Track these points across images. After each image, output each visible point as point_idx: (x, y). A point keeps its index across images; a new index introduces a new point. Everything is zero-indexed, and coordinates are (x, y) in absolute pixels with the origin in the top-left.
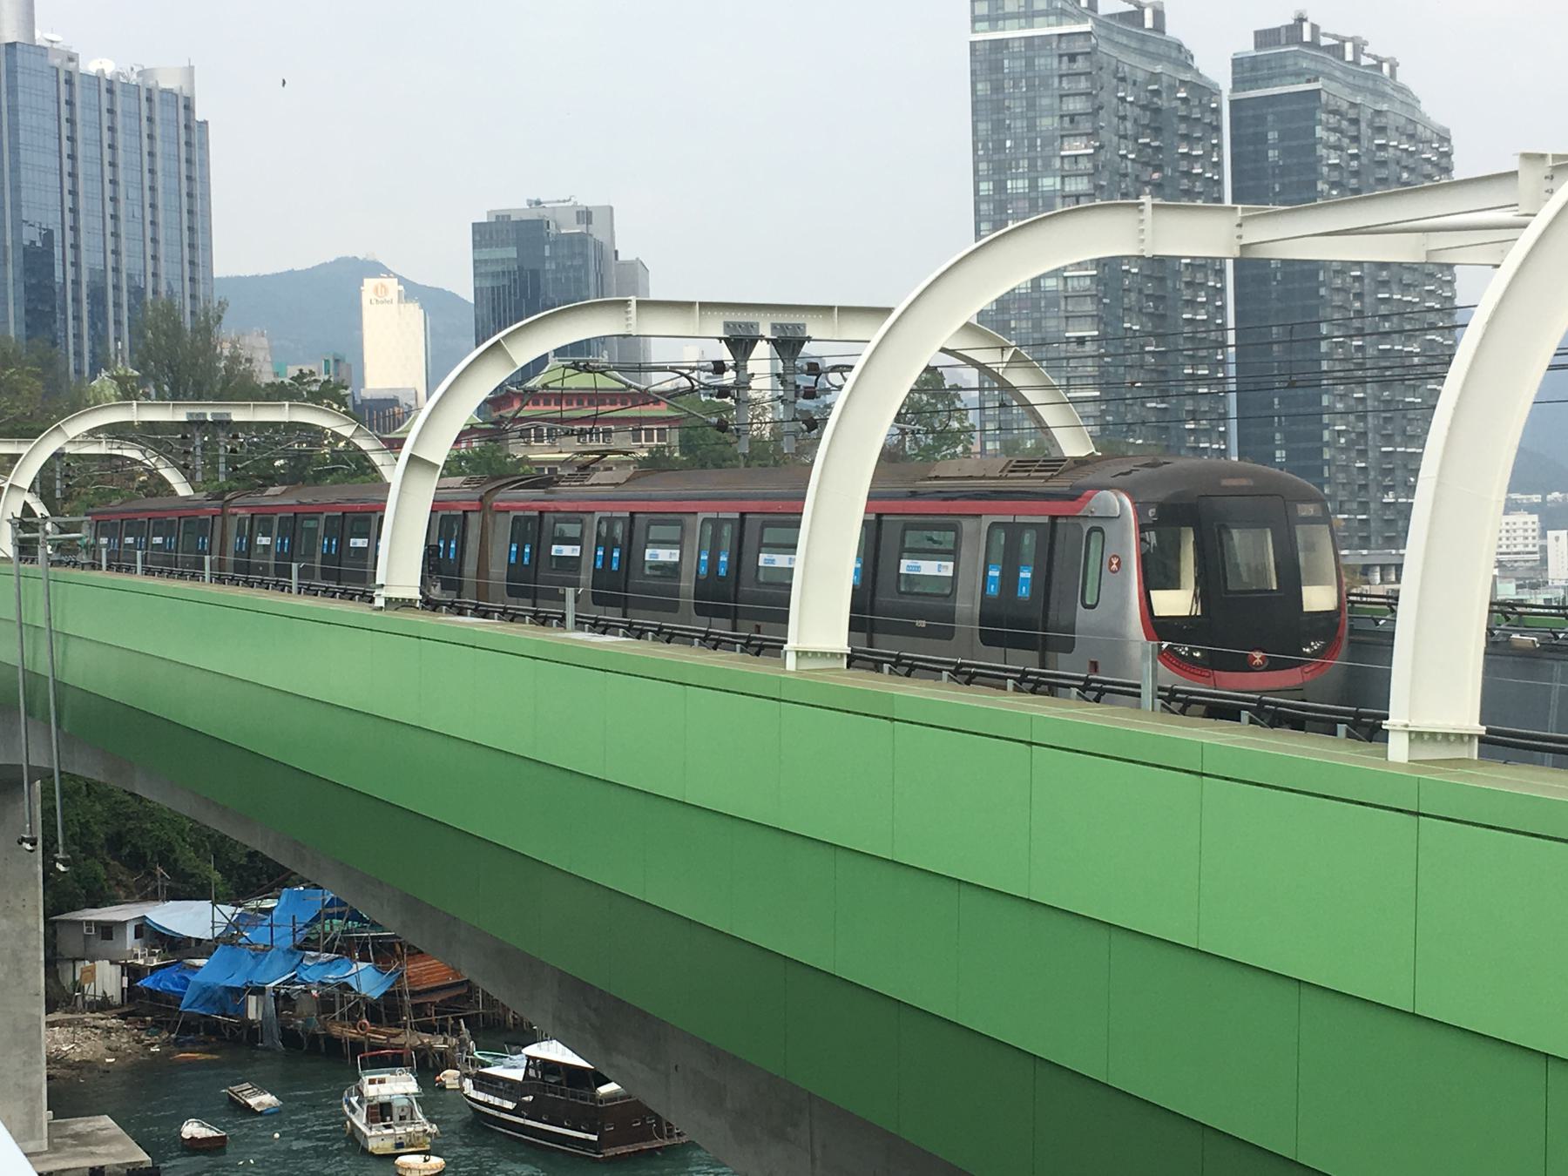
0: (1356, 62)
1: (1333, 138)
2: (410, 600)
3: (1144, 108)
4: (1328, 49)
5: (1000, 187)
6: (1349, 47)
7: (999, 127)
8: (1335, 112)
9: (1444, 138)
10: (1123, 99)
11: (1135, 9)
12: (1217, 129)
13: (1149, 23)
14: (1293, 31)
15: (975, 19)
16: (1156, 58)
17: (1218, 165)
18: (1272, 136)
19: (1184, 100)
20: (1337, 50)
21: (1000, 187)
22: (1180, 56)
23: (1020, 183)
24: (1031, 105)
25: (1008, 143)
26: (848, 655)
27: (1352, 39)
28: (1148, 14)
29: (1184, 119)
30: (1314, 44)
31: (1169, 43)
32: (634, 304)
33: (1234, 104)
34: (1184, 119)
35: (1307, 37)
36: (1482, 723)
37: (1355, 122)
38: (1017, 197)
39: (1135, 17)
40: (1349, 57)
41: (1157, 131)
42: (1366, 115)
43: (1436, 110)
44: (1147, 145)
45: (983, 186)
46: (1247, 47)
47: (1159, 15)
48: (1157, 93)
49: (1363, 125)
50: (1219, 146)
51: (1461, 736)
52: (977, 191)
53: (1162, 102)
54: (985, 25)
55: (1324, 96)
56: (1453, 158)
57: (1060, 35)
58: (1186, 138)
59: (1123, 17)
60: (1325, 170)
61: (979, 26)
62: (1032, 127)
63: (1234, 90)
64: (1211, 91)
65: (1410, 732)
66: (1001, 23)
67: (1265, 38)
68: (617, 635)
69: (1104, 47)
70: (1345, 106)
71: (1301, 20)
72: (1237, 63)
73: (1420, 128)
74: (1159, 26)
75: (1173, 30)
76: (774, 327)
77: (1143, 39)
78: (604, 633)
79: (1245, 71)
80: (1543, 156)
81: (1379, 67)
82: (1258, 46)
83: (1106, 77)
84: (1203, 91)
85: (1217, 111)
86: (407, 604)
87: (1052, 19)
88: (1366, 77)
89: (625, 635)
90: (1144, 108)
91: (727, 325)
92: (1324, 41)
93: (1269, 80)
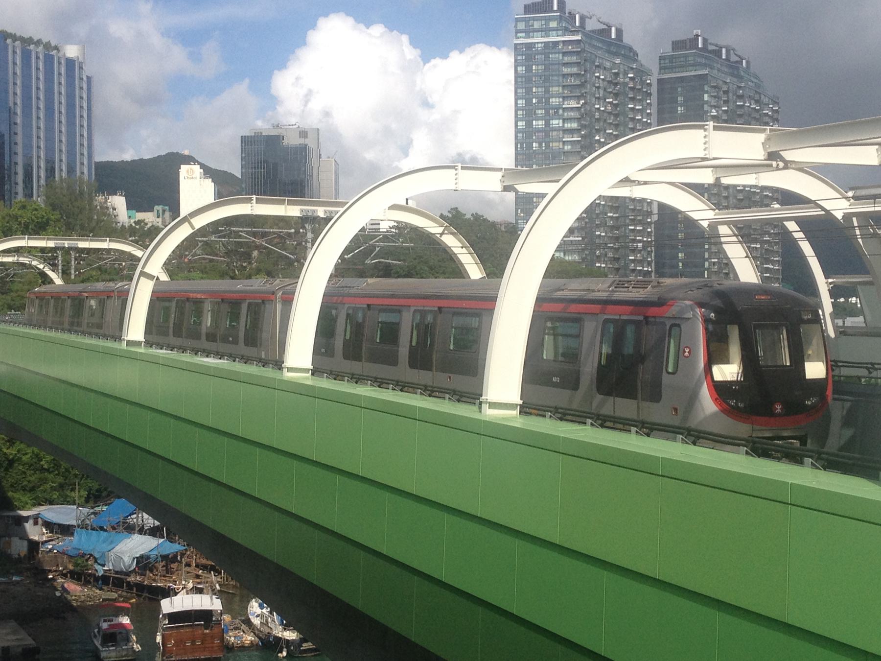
2: (139, 342)
3: (610, 82)
5: (529, 124)
6: (724, 51)
7: (529, 91)
10: (598, 77)
11: (606, 27)
13: (613, 36)
15: (517, 32)
22: (630, 54)
23: (540, 122)
25: (534, 101)
26: (312, 370)
28: (613, 30)
31: (624, 47)
33: (660, 81)
34: (632, 89)
36: (521, 399)
38: (539, 131)
39: (606, 32)
45: (520, 123)
46: (668, 49)
47: (619, 32)
49: (731, 95)
51: (513, 404)
53: (621, 79)
54: (523, 35)
55: (709, 77)
57: (564, 42)
58: (633, 99)
59: (601, 32)
61: (519, 35)
62: (547, 91)
64: (648, 73)
65: (489, 403)
66: (531, 34)
67: (677, 45)
68: (224, 359)
71: (697, 36)
73: (762, 97)
75: (627, 39)
76: (325, 212)
77: (610, 44)
78: (220, 359)
79: (666, 63)
80: (502, 169)
84: (641, 72)
86: (137, 344)
87: (560, 32)
89: (227, 359)
92: (711, 48)
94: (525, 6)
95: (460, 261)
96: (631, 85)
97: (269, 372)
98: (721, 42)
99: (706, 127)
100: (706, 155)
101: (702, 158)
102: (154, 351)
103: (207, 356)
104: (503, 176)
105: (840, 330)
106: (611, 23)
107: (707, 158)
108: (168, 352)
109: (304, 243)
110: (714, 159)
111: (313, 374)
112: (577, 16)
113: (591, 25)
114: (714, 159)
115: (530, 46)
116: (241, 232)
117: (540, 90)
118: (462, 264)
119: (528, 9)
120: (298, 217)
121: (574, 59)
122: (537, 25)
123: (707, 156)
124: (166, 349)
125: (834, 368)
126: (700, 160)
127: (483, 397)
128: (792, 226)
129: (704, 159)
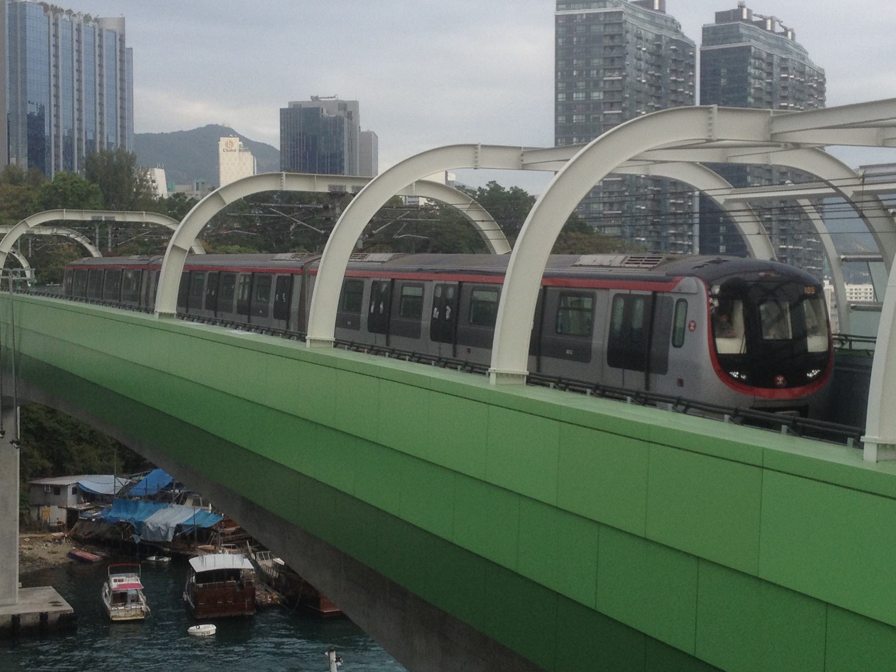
0: (772, 31)
1: (757, 72)
4: (757, 23)
5: (569, 97)
6: (769, 22)
8: (760, 58)
9: (823, 76)
10: (640, 49)
12: (693, 67)
14: (736, 14)
16: (661, 27)
17: (692, 88)
18: (723, 71)
19: (675, 51)
20: (762, 24)
21: (569, 97)
23: (581, 95)
25: (575, 73)
26: (334, 342)
27: (771, 18)
30: (748, 21)
32: (284, 176)
33: (702, 53)
34: (675, 61)
35: (745, 17)
36: (527, 370)
37: (770, 64)
40: (769, 28)
41: (659, 67)
42: (776, 60)
43: (817, 58)
44: (653, 75)
45: (560, 96)
46: (711, 21)
48: (659, 46)
50: (694, 76)
53: (663, 51)
54: (564, 6)
55: (753, 50)
56: (826, 85)
57: (605, 14)
58: (674, 71)
60: (752, 91)
61: (560, 6)
62: (588, 63)
64: (690, 46)
65: (497, 373)
66: (573, 6)
67: (720, 16)
69: (630, 20)
70: (764, 55)
71: (741, 7)
72: (706, 30)
73: (807, 69)
74: (662, 9)
77: (653, 17)
78: (248, 331)
81: (785, 34)
82: (717, 20)
83: (629, 37)
84: (685, 46)
85: (693, 57)
86: (170, 316)
88: (777, 39)
90: (651, 54)
91: (330, 187)
92: (755, 19)
95: (485, 236)
97: (292, 344)
98: (766, 14)
99: (711, 110)
100: (711, 136)
101: (707, 140)
103: (236, 328)
104: (522, 155)
105: (852, 305)
107: (711, 140)
108: (199, 324)
109: (332, 218)
110: (719, 140)
111: (335, 346)
114: (719, 140)
115: (570, 18)
116: (271, 207)
117: (580, 62)
118: (488, 239)
120: (328, 193)
121: (616, 30)
123: (712, 138)
124: (197, 322)
125: (844, 342)
126: (704, 141)
127: (491, 368)
128: (803, 202)
129: (709, 141)
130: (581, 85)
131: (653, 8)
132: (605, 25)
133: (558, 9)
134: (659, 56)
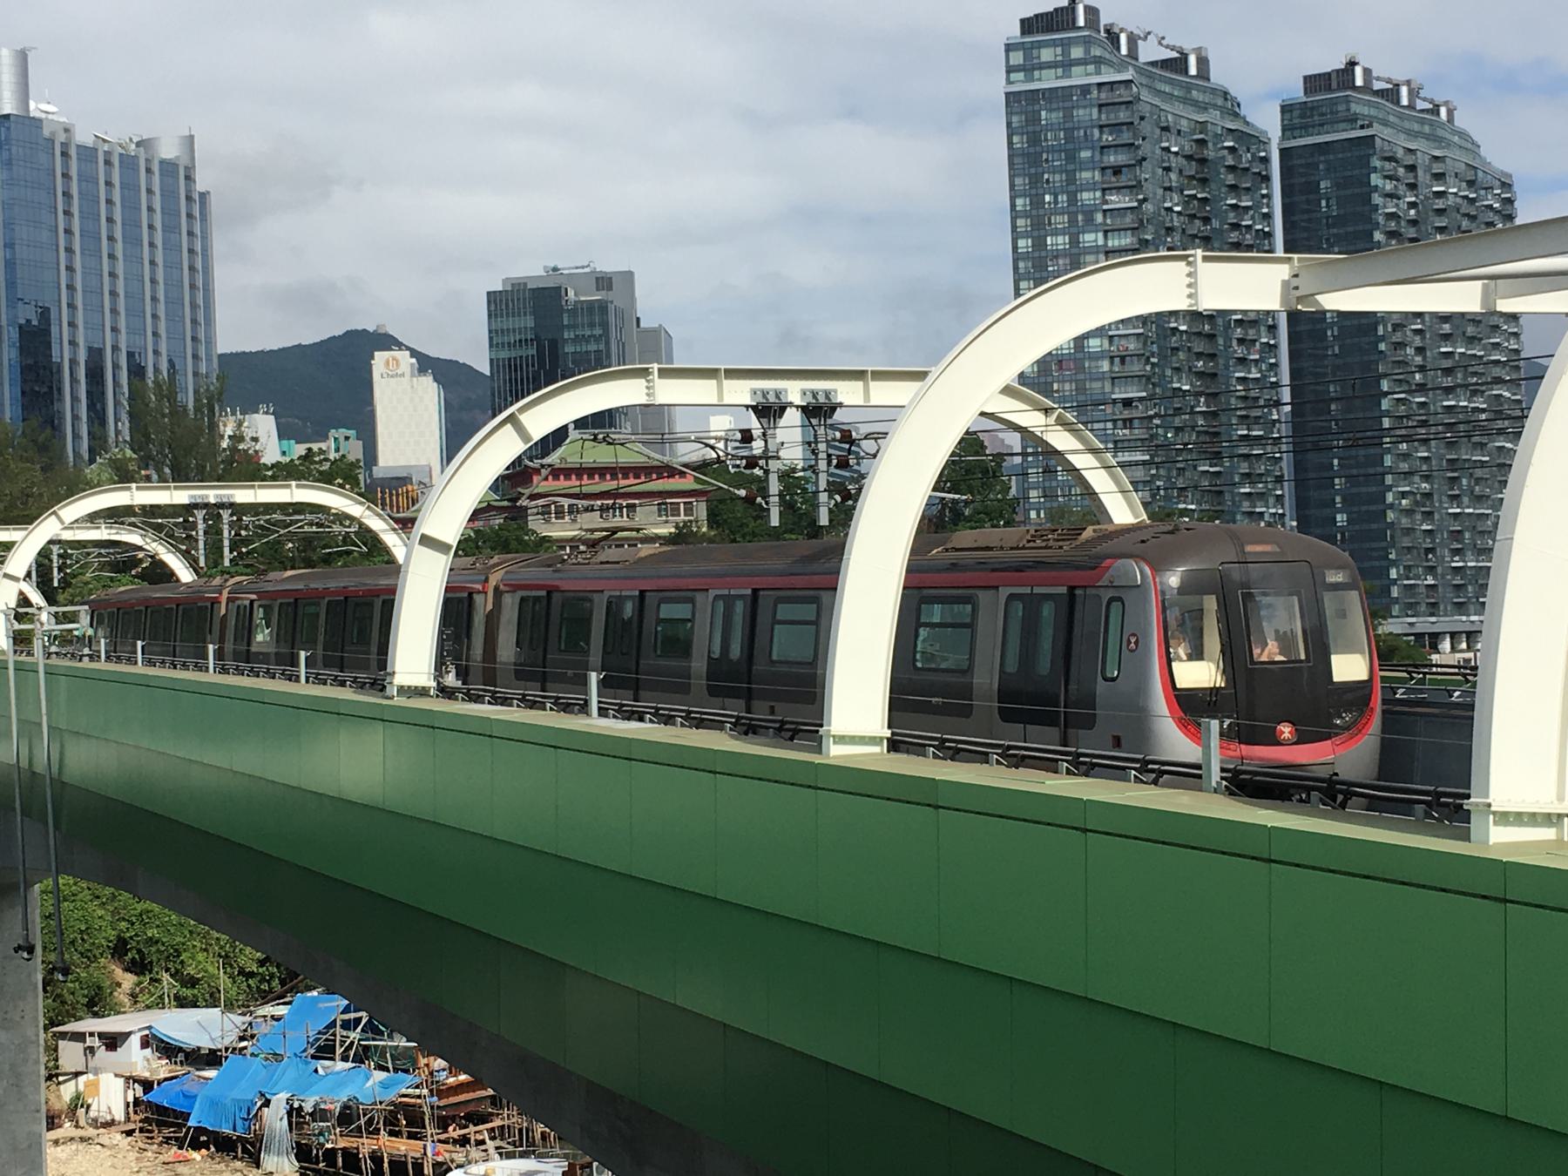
0: (1411, 107)
3: (1189, 158)
5: (1039, 244)
6: (1404, 90)
7: (1035, 180)
9: (1507, 186)
10: (1167, 150)
11: (1175, 55)
12: (1267, 179)
13: (1193, 71)
15: (1010, 70)
16: (1203, 107)
17: (1268, 217)
19: (1232, 150)
20: (1392, 94)
21: (1039, 244)
22: (1228, 103)
23: (1060, 239)
24: (1071, 157)
25: (1047, 198)
28: (1192, 60)
29: (1232, 169)
30: (1367, 88)
31: (1214, 91)
33: (1284, 153)
34: (1232, 169)
35: (1359, 82)
37: (1412, 168)
38: (1056, 255)
39: (1177, 64)
40: (1405, 102)
41: (1204, 182)
42: (1422, 160)
44: (1194, 197)
45: (1021, 243)
46: (1297, 92)
47: (1203, 62)
48: (1202, 142)
49: (1420, 172)
50: (1268, 196)
52: (1015, 248)
53: (1210, 153)
54: (1021, 76)
55: (1378, 141)
56: (1516, 204)
57: (1100, 85)
58: (1233, 188)
59: (1165, 64)
60: (1381, 220)
61: (1013, 76)
62: (1071, 180)
63: (1284, 138)
64: (1263, 143)
66: (1036, 73)
67: (1314, 83)
69: (1145, 96)
70: (1400, 153)
71: (1352, 64)
72: (1286, 109)
73: (1480, 174)
75: (1217, 77)
77: (1188, 88)
79: (1295, 116)
81: (1435, 111)
83: (1146, 128)
84: (1250, 139)
85: (1266, 161)
87: (1091, 68)
88: (1422, 122)
90: (1189, 158)
92: (1378, 86)
93: (1321, 127)
94: (1023, 21)
96: (1230, 161)
98: (1398, 77)
102: (460, 706)
106: (1187, 46)
112: (1123, 38)
113: (1150, 52)
119: (1028, 26)
121: (1123, 116)
122: (1047, 55)
130: (1061, 221)
131: (1186, 71)
132: (1100, 106)
133: (1009, 82)
134: (1203, 161)
